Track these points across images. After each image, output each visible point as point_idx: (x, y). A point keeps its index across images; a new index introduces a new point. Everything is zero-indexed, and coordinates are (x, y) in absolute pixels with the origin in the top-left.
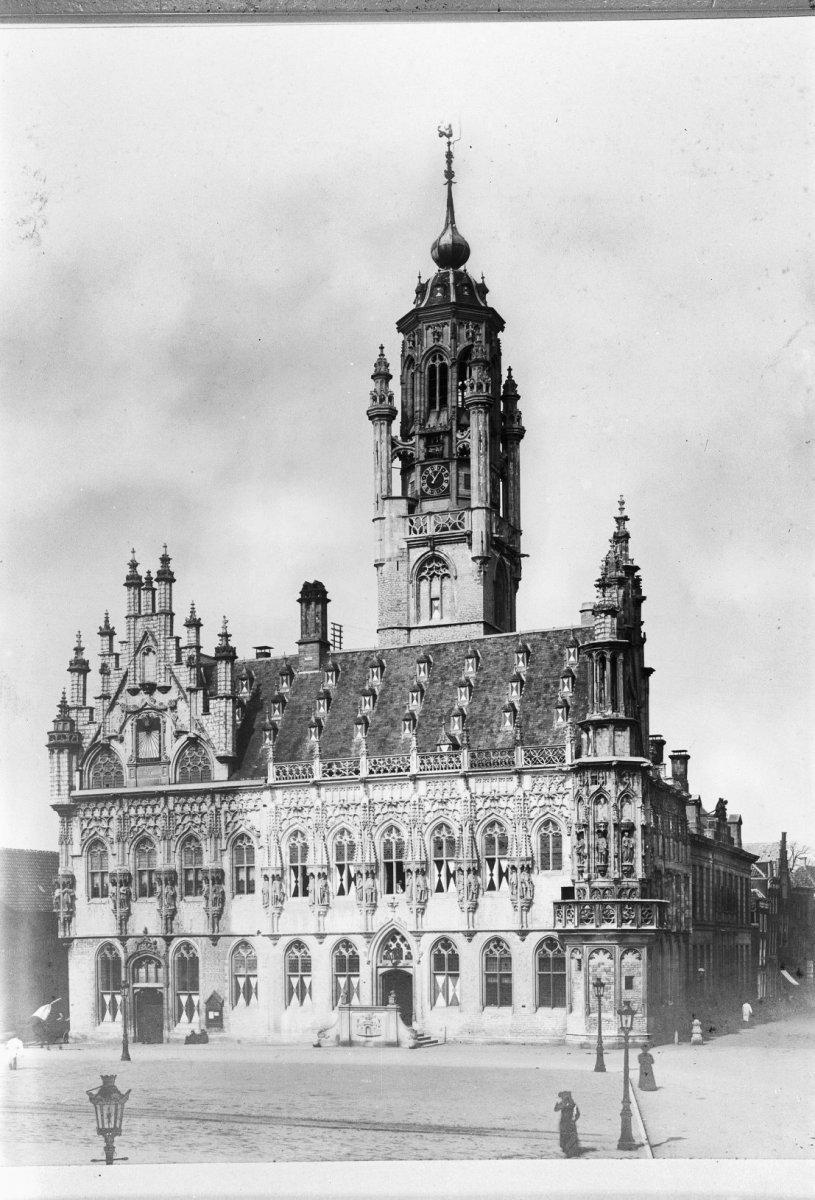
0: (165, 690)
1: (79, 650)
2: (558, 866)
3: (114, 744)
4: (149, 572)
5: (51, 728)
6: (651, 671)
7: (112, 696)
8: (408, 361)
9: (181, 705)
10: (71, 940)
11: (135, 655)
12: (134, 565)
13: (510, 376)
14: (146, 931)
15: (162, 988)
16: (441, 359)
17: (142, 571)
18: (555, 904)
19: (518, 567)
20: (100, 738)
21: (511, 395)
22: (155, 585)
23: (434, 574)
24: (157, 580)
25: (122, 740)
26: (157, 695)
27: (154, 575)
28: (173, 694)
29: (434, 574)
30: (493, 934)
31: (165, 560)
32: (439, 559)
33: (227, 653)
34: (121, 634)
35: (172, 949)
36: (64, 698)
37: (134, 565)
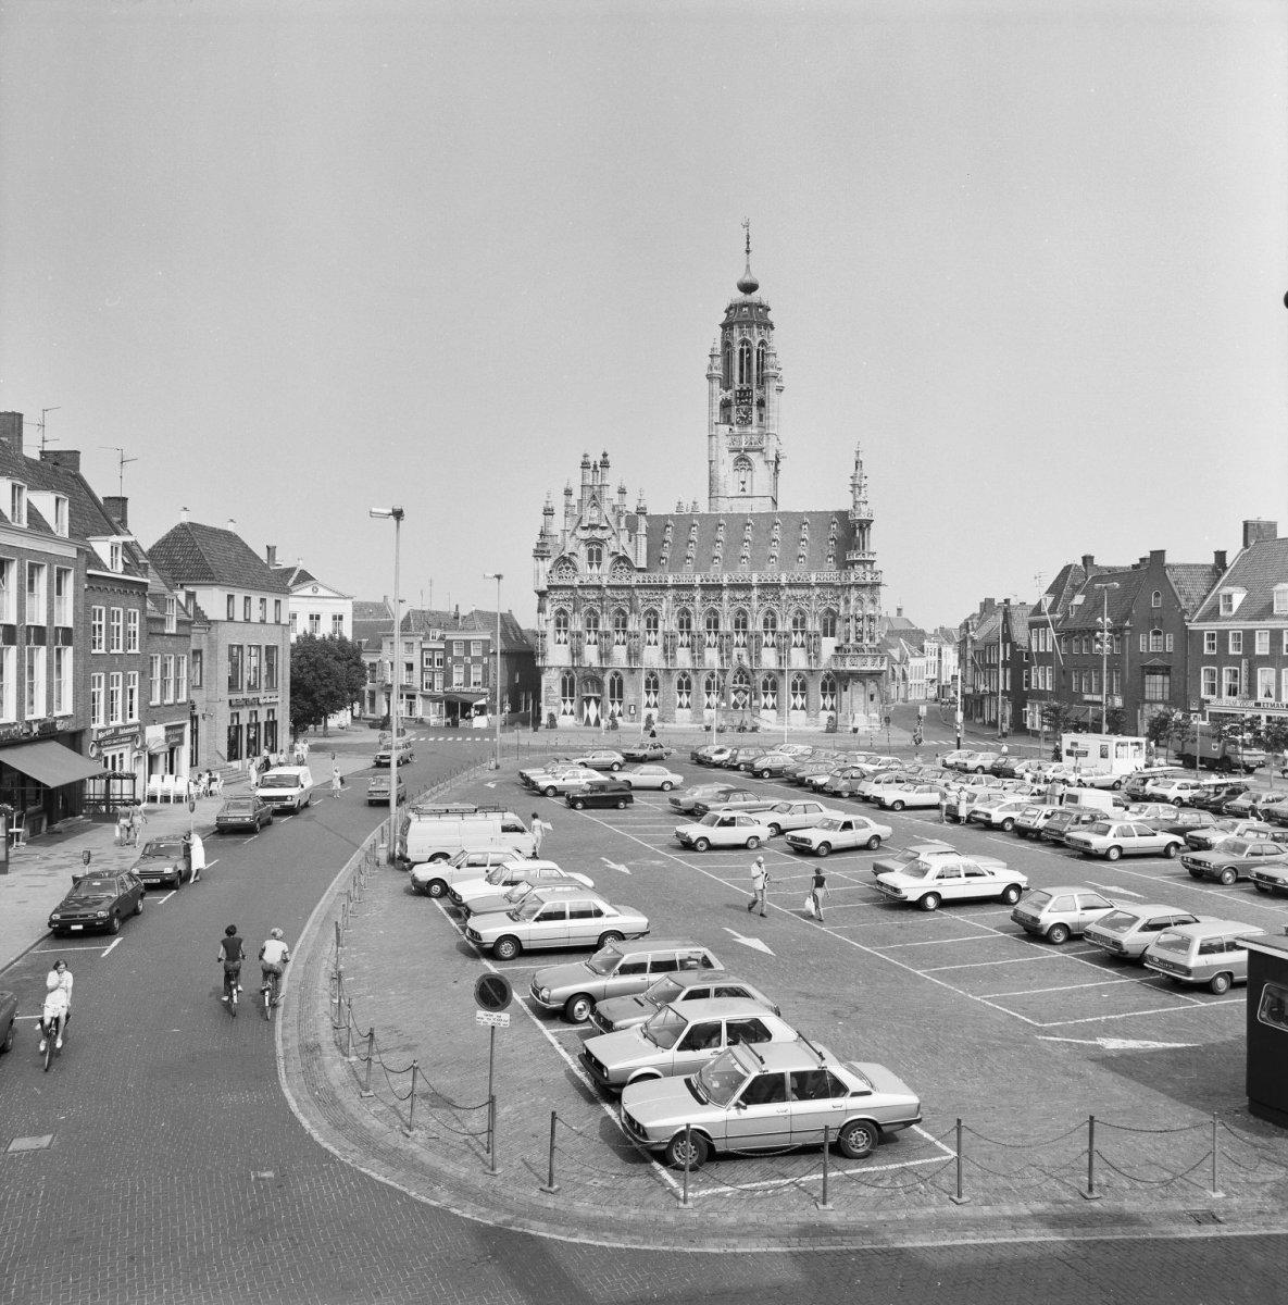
0: (603, 528)
3: (574, 558)
17: (591, 460)
22: (599, 469)
31: (605, 455)
32: (746, 460)
34: (577, 494)
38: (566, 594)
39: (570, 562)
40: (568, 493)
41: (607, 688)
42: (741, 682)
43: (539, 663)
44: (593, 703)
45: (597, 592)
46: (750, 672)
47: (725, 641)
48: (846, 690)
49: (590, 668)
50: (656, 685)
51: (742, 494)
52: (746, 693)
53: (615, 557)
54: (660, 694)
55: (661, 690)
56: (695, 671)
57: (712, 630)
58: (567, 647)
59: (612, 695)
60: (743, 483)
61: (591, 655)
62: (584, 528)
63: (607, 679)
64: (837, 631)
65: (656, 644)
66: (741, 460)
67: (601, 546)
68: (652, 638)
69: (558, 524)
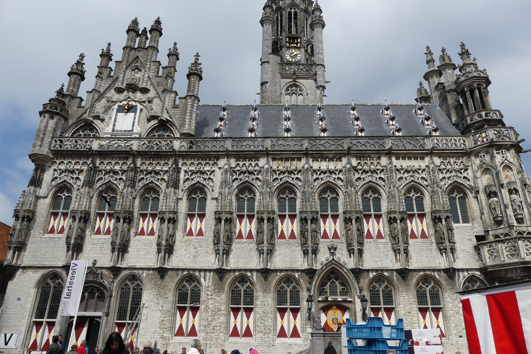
0: (145, 91)
2: (466, 220)
3: (97, 122)
7: (102, 92)
9: (156, 101)
12: (135, 22)
15: (100, 317)
16: (294, 9)
20: (85, 116)
23: (294, 93)
25: (103, 120)
27: (148, 29)
28: (152, 94)
29: (294, 93)
30: (422, 273)
32: (297, 86)
33: (195, 74)
36: (62, 88)
37: (135, 22)
40: (106, 55)
41: (114, 304)
42: (334, 292)
46: (351, 277)
47: (309, 226)
50: (196, 297)
53: (154, 122)
55: (202, 307)
58: (64, 236)
59: (121, 315)
62: (119, 91)
65: (200, 233)
66: (291, 86)
68: (195, 225)
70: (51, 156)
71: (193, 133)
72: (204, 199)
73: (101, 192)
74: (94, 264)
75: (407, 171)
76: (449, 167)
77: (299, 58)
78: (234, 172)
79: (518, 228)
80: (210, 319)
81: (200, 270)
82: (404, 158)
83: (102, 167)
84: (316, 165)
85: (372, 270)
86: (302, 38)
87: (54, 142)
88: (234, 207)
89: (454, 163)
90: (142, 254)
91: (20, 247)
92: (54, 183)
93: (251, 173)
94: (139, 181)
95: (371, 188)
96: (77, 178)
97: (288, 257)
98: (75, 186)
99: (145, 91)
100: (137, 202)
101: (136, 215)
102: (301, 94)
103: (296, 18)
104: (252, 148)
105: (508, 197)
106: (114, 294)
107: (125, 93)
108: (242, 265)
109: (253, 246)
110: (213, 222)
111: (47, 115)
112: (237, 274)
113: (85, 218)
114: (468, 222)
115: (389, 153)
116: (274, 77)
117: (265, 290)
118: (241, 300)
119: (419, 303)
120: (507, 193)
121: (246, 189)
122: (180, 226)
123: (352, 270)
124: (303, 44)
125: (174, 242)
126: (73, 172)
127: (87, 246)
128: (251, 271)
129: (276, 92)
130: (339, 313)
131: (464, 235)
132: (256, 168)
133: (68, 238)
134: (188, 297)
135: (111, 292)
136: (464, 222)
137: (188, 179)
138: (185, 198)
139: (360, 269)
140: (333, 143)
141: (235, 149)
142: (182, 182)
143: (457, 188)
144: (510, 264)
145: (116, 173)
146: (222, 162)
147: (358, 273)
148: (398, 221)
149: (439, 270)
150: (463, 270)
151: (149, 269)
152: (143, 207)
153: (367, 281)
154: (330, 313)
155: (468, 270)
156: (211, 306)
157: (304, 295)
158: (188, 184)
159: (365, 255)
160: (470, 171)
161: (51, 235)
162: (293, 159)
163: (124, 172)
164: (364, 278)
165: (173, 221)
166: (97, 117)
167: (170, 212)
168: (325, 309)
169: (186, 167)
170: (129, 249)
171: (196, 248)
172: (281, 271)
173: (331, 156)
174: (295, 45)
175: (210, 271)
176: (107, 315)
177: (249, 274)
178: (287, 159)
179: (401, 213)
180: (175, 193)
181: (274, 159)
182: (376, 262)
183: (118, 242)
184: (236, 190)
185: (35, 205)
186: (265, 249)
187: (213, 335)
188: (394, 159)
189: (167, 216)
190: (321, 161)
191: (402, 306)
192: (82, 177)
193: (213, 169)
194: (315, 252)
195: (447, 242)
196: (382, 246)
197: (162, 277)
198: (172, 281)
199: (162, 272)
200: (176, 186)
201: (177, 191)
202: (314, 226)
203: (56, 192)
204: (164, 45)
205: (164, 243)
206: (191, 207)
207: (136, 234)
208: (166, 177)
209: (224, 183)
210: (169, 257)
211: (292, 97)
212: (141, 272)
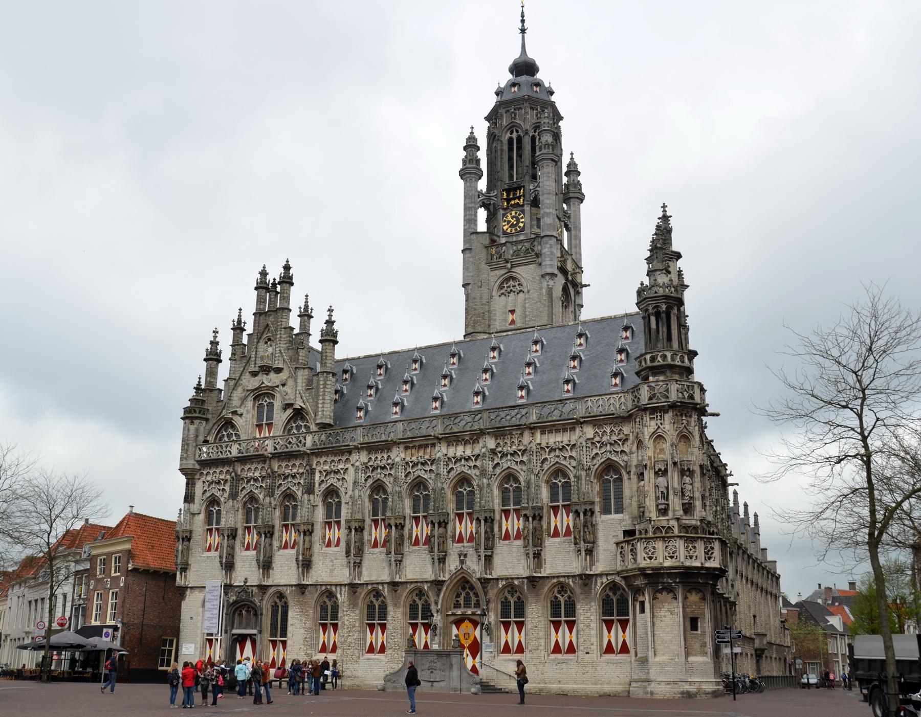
0: (279, 370)
1: (214, 343)
2: (619, 510)
4: (274, 279)
5: (188, 404)
6: (695, 353)
8: (492, 137)
9: (290, 383)
10: (185, 588)
11: (258, 342)
12: (264, 274)
13: (572, 159)
14: (246, 581)
16: (517, 132)
17: (270, 279)
18: (617, 544)
19: (578, 293)
20: (224, 413)
21: (573, 170)
22: (278, 289)
24: (279, 283)
26: (272, 375)
27: (278, 280)
28: (284, 375)
30: (555, 580)
31: (287, 268)
32: (514, 279)
33: (330, 338)
35: (266, 597)
37: (264, 274)
38: (221, 474)
39: (233, 426)
41: (267, 621)
42: (467, 605)
43: (180, 581)
44: (248, 645)
45: (259, 467)
46: (478, 586)
48: (643, 611)
49: (244, 589)
51: (512, 327)
52: (475, 624)
53: (289, 411)
54: (339, 631)
55: (340, 623)
56: (394, 585)
57: (421, 514)
58: (217, 554)
60: (512, 312)
61: (246, 572)
62: (254, 374)
63: (266, 605)
64: (626, 502)
66: (507, 280)
67: (273, 396)
69: (224, 370)
70: (197, 467)
71: (328, 421)
72: (339, 504)
73: (245, 503)
74: (246, 582)
75: (552, 450)
76: (605, 439)
77: (521, 225)
78: (367, 467)
79: (657, 523)
80: (346, 635)
81: (336, 585)
82: (550, 432)
83: (244, 475)
84: (451, 452)
85: (502, 579)
86: (527, 187)
87: (198, 451)
88: (367, 511)
89: (609, 433)
90: (285, 572)
91: (184, 569)
92: (204, 498)
93: (383, 468)
94: (278, 487)
95: (510, 476)
96: (223, 490)
97: (418, 567)
98: (222, 499)
99: (279, 370)
100: (277, 513)
101: (277, 528)
102: (521, 291)
103: (519, 148)
104: (384, 438)
105: (653, 481)
106: (264, 612)
107: (260, 374)
108: (374, 578)
109: (383, 556)
110: (346, 531)
111: (187, 421)
112: (370, 587)
113: (233, 534)
114: (622, 512)
115: (532, 428)
116: (478, 271)
117: (396, 605)
118: (376, 616)
119: (553, 615)
120: (652, 475)
121: (378, 487)
122: (317, 537)
123: (479, 579)
124: (527, 196)
125: (311, 556)
126: (219, 483)
127: (238, 565)
128: (382, 584)
129: (481, 297)
130: (470, 625)
131: (610, 527)
132: (389, 461)
133: (221, 557)
134: (328, 616)
135: (261, 609)
136: (617, 512)
137: (323, 481)
138: (320, 504)
139: (488, 581)
140: (469, 419)
141: (366, 440)
142: (317, 485)
143: (610, 467)
144: (631, 570)
145: (256, 480)
146: (354, 457)
147: (485, 582)
148: (530, 519)
149: (573, 576)
150: (601, 575)
151: (292, 586)
152: (285, 517)
153: (495, 591)
154: (463, 626)
155: (607, 575)
156: (346, 623)
157: (433, 608)
158: (324, 486)
159: (497, 561)
160: (630, 442)
161: (209, 554)
162: (426, 446)
163: (263, 478)
164: (492, 588)
165: (309, 533)
166: (235, 413)
167: (304, 524)
168: (458, 623)
169: (322, 465)
170: (274, 565)
171: (332, 561)
172: (412, 583)
173: (467, 438)
174: (517, 201)
175: (345, 585)
176: (260, 632)
177: (380, 587)
178: (420, 447)
179: (533, 508)
180: (309, 500)
181: (406, 448)
182: (507, 569)
183: (261, 558)
184: (368, 492)
185: (191, 523)
186: (393, 559)
187: (348, 652)
188: (538, 435)
189: (302, 528)
190: (457, 445)
191: (529, 619)
192: (227, 488)
193: (347, 466)
194: (442, 560)
195: (582, 542)
196: (515, 550)
197: (303, 593)
198: (312, 598)
199: (302, 588)
200: (310, 490)
201: (312, 497)
202: (442, 530)
203: (208, 506)
204: (296, 303)
205: (301, 558)
206: (328, 515)
207: (280, 548)
208: (302, 482)
209: (355, 483)
210: (308, 572)
211: (510, 298)
212: (285, 588)
